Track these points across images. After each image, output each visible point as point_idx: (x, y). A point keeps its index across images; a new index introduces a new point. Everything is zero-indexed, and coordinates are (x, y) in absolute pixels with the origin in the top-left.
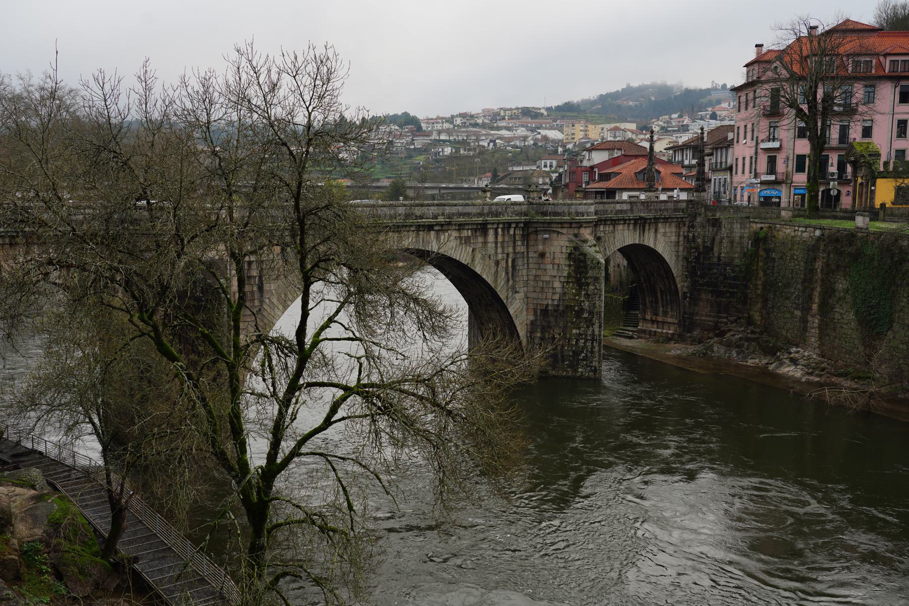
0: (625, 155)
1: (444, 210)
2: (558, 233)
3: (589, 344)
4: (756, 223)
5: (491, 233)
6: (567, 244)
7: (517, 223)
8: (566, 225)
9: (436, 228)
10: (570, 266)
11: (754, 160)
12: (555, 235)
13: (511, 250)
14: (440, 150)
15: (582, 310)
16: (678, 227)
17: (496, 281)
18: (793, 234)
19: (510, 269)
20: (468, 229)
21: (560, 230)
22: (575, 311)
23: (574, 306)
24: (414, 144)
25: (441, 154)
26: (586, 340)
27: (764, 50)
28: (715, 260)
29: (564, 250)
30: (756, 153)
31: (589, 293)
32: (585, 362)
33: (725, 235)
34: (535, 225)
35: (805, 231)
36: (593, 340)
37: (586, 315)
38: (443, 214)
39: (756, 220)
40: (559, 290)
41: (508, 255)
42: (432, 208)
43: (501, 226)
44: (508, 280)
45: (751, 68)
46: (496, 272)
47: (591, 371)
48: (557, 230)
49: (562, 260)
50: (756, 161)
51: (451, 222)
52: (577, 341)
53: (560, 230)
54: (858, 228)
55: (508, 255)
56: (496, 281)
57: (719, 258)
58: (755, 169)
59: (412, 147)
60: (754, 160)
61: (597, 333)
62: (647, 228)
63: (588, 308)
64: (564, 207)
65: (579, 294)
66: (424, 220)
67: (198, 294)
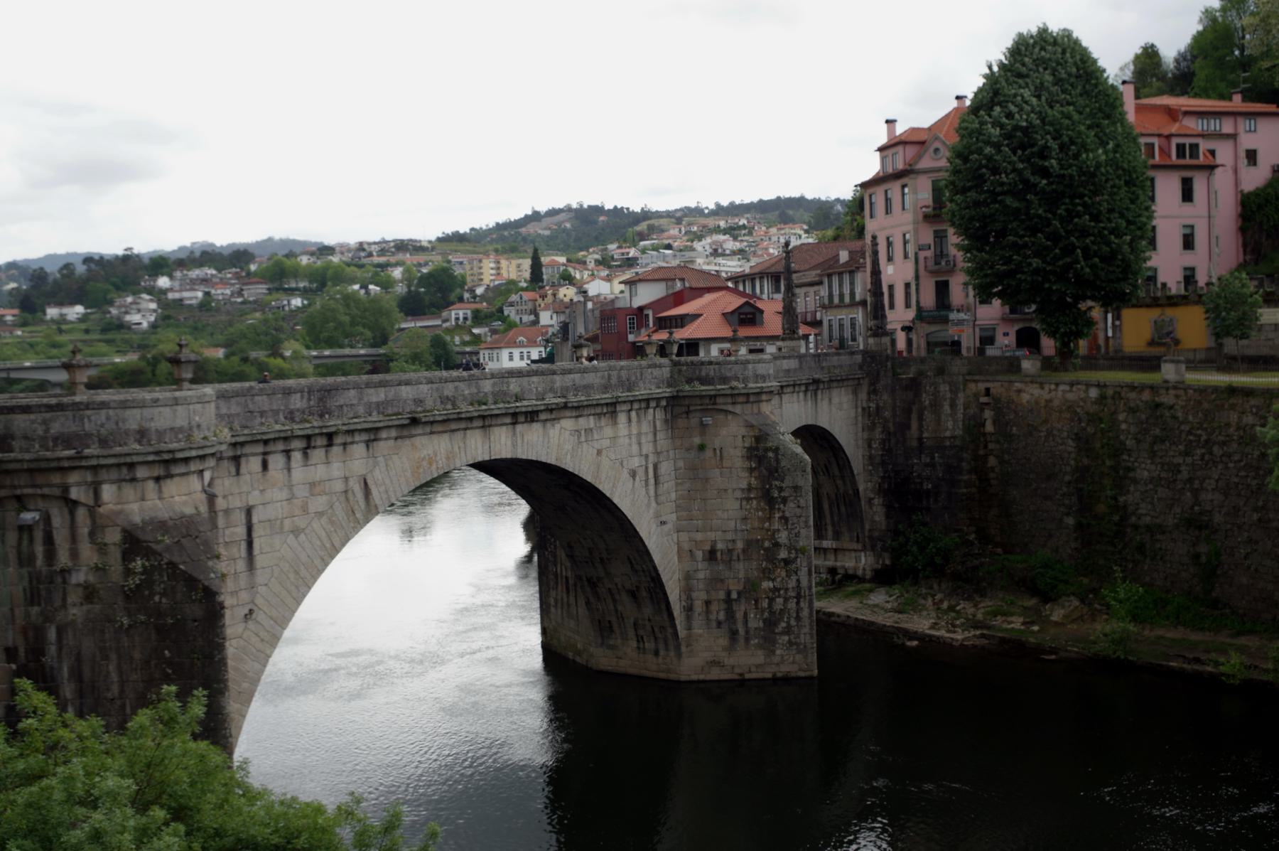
0: (691, 288)
1: (553, 382)
2: (726, 411)
3: (792, 605)
4: (976, 381)
5: (622, 418)
6: (743, 431)
7: (658, 400)
8: (741, 399)
10: (751, 470)
11: (913, 287)
12: (721, 417)
14: (285, 302)
15: (777, 545)
16: (855, 393)
18: (1047, 397)
19: (652, 481)
21: (730, 408)
22: (765, 549)
23: (763, 540)
24: (243, 296)
25: (287, 308)
26: (786, 600)
27: (900, 129)
28: (915, 443)
29: (739, 442)
30: (917, 277)
31: (787, 514)
32: (786, 638)
33: (927, 402)
34: (687, 402)
35: (1071, 391)
36: (798, 597)
37: (783, 554)
38: (552, 390)
39: (977, 378)
41: (647, 456)
42: (535, 379)
45: (889, 152)
47: (799, 652)
48: (724, 407)
49: (736, 457)
50: (917, 290)
51: (566, 403)
52: (771, 600)
54: (1166, 381)
57: (920, 439)
58: (918, 302)
59: (239, 300)
60: (913, 287)
61: (804, 583)
62: (819, 396)
63: (786, 541)
64: (736, 367)
65: (770, 519)
66: (525, 403)
67: (157, 598)
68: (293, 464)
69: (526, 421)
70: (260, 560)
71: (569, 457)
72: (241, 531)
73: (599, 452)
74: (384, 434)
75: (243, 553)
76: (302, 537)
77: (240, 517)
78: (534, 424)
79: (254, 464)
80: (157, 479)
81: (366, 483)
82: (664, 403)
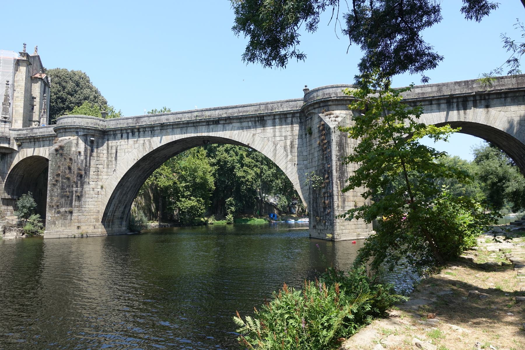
8: (316, 106)
9: (222, 122)
13: (289, 133)
17: (275, 155)
20: (248, 122)
21: (313, 111)
40: (316, 158)
41: (286, 137)
43: (277, 117)
44: (287, 156)
46: (275, 149)
48: (311, 111)
53: (313, 111)
55: (286, 137)
56: (275, 155)
68: (129, 136)
69: (213, 124)
70: (118, 158)
71: (236, 136)
72: (114, 151)
73: (254, 135)
74: (156, 128)
75: (114, 156)
76: (130, 154)
77: (114, 148)
78: (219, 125)
79: (119, 136)
80: (64, 132)
81: (150, 142)
82: (298, 115)
